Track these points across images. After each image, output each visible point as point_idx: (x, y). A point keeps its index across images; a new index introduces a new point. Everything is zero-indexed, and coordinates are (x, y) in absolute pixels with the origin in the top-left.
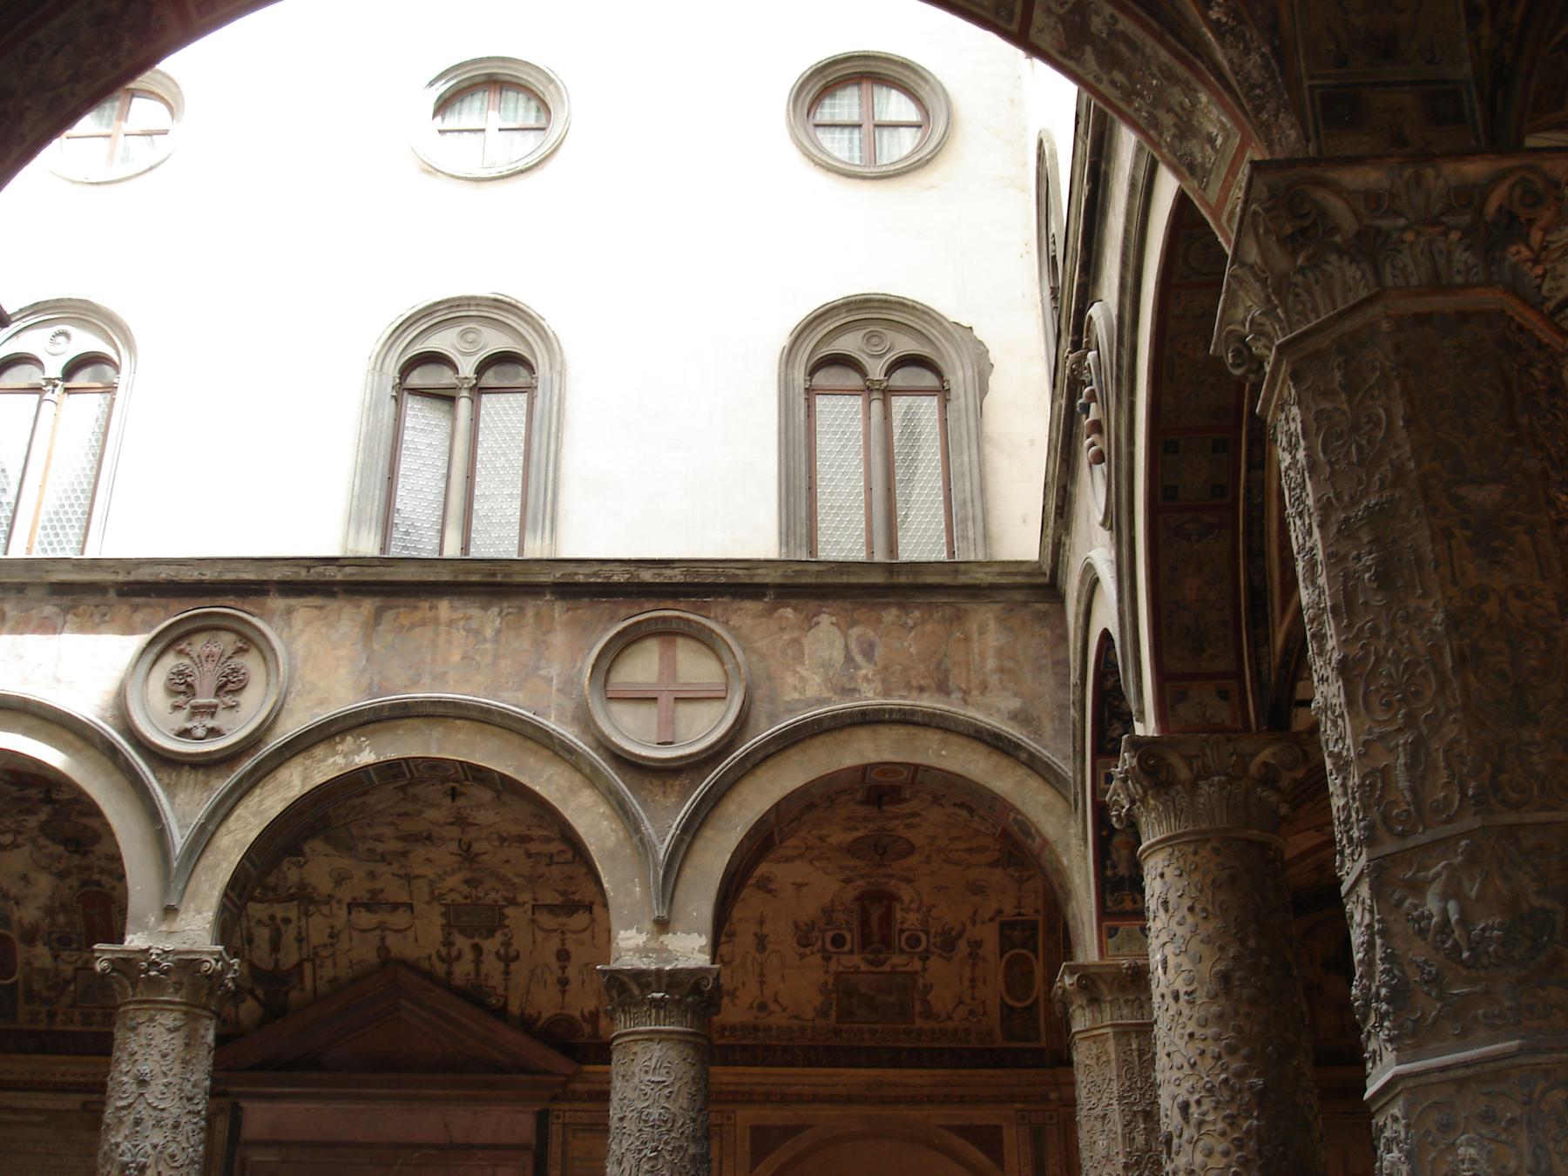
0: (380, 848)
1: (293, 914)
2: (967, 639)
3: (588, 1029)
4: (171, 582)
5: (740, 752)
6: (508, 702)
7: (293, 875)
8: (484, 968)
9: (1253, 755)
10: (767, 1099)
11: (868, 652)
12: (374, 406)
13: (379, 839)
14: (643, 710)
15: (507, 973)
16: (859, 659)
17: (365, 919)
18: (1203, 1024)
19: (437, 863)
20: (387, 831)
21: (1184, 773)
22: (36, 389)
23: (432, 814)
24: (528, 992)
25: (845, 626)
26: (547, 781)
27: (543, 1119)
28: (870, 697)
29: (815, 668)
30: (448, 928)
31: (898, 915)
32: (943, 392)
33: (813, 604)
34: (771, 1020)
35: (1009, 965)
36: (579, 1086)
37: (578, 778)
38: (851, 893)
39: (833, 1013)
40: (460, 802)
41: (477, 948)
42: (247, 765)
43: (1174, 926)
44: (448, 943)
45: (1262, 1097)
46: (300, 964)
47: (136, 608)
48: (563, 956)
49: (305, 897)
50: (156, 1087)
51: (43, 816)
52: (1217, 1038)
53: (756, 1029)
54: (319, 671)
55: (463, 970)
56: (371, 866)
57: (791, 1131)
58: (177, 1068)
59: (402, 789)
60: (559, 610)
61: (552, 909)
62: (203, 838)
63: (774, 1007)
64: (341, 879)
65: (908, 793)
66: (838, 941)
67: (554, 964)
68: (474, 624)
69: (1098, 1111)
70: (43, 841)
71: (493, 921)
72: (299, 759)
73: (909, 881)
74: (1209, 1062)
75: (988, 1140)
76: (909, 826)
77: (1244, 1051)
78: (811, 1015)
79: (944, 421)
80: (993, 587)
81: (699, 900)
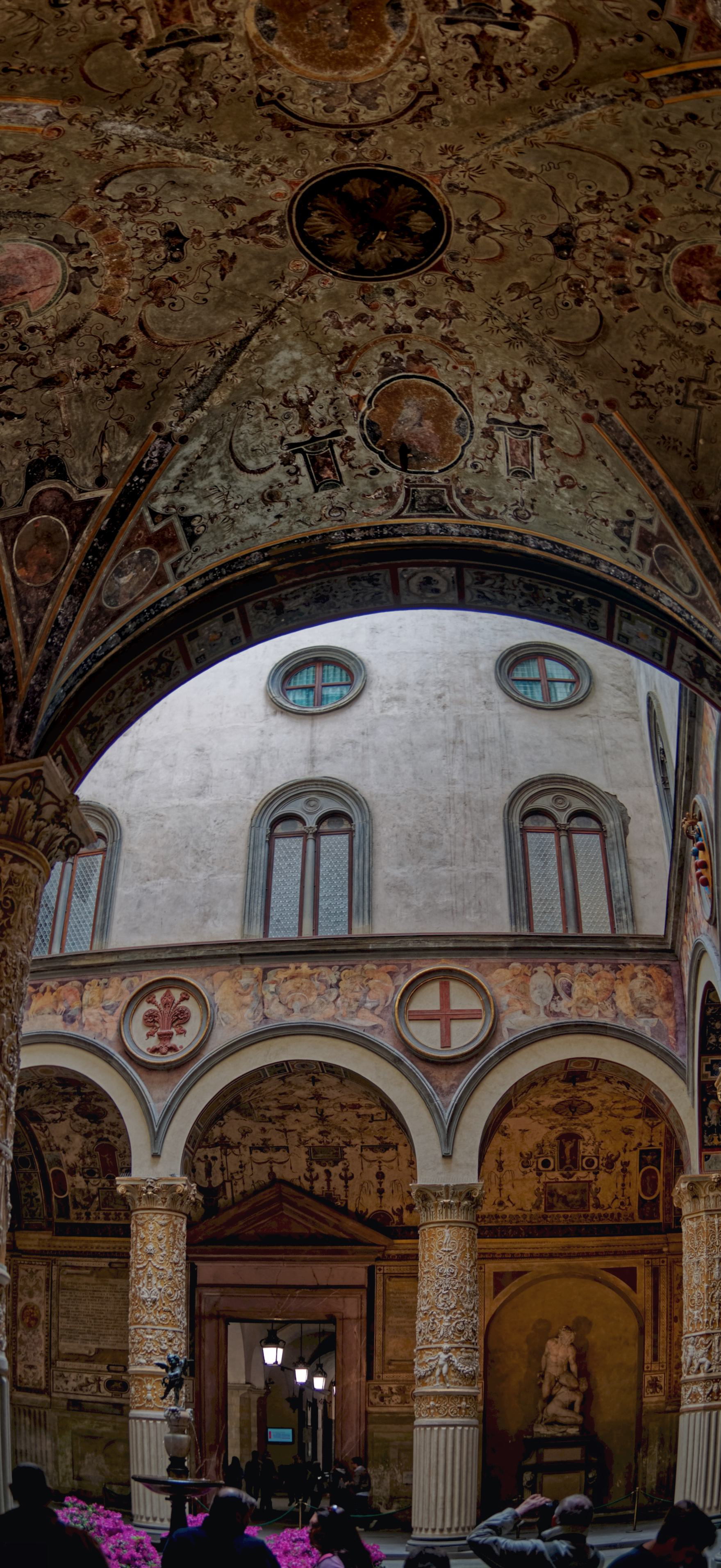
0: (268, 1114)
3: (396, 1219)
8: (332, 1184)
10: (503, 1257)
13: (267, 1108)
15: (346, 1187)
17: (260, 1156)
19: (303, 1122)
30: (310, 1161)
31: (581, 1147)
32: (602, 832)
34: (506, 1212)
36: (392, 1252)
38: (554, 1135)
41: (328, 1173)
44: (311, 1170)
48: (380, 1176)
49: (224, 1144)
53: (497, 1216)
55: (319, 1187)
56: (263, 1125)
61: (372, 1148)
62: (170, 1112)
63: (507, 1203)
64: (245, 1134)
65: (590, 1076)
66: (546, 1164)
67: (375, 1180)
71: (337, 1156)
76: (590, 1095)
78: (529, 1207)
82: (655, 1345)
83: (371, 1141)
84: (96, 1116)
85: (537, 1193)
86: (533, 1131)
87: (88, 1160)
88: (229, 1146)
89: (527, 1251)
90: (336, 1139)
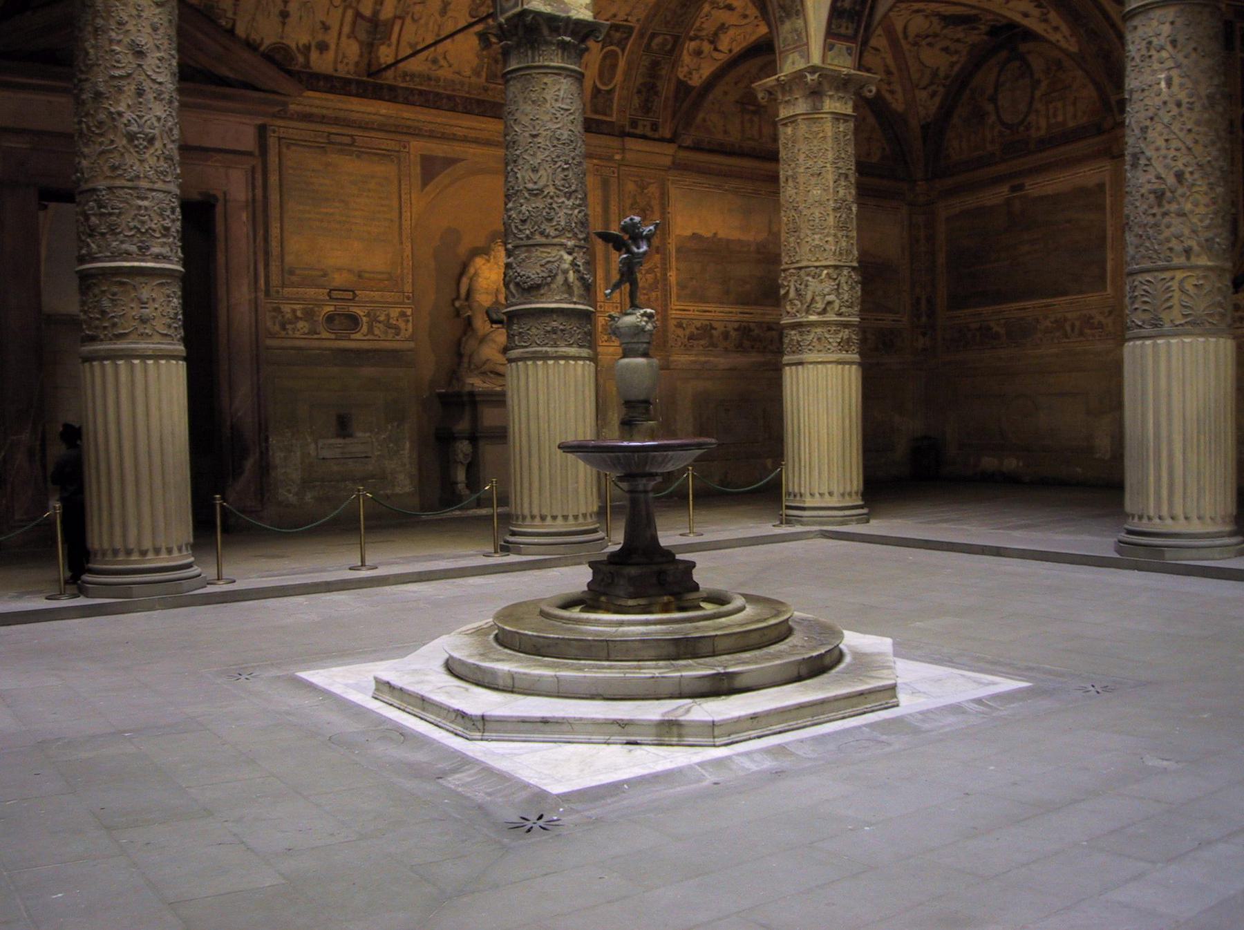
10: (432, 136)
24: (253, 19)
27: (262, 131)
34: (440, 73)
35: (604, 58)
39: (484, 74)
43: (1180, 57)
50: (151, 61)
52: (1206, 134)
53: (429, 79)
57: (450, 162)
63: (443, 62)
69: (815, 169)
89: (473, 134)
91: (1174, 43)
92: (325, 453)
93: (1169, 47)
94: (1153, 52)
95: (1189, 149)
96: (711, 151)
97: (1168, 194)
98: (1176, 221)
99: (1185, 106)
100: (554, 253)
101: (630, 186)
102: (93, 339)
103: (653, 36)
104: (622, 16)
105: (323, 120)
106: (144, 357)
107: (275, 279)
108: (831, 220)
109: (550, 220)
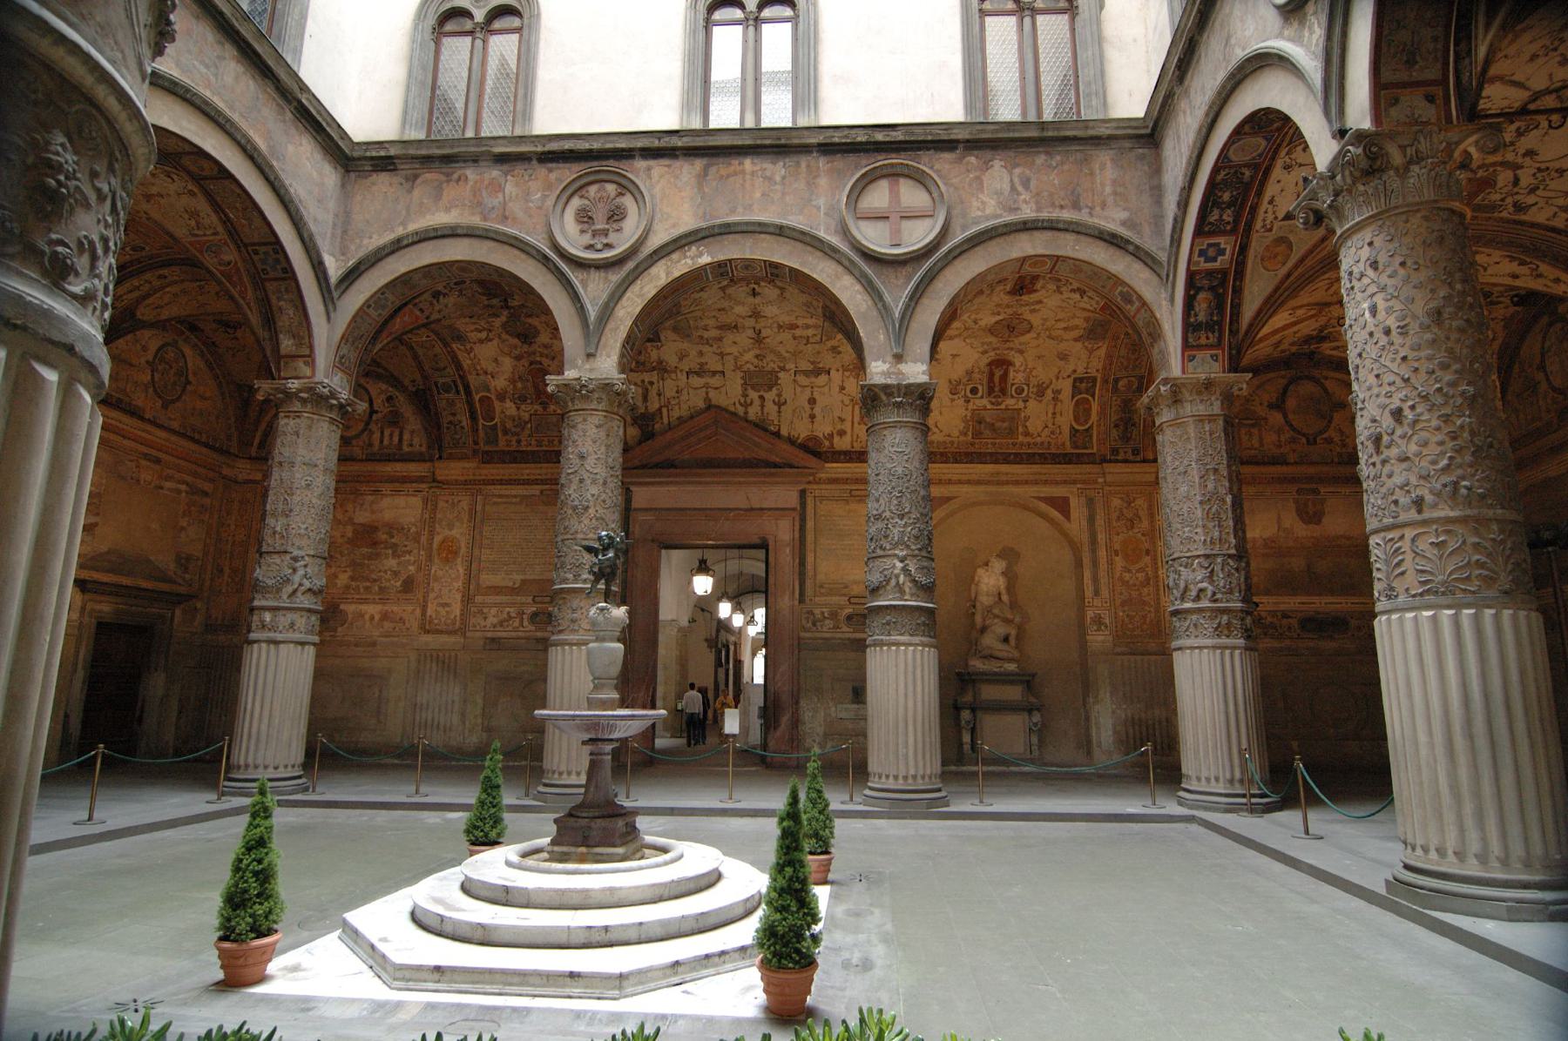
0: (706, 335)
1: (655, 379)
2: (1092, 174)
4: (571, 151)
5: (945, 249)
6: (795, 221)
7: (654, 354)
9: (1458, 143)
11: (1026, 183)
12: (694, 32)
14: (881, 224)
16: (1020, 188)
17: (696, 381)
18: (1417, 348)
19: (739, 345)
20: (712, 322)
21: (1397, 158)
22: (471, 33)
23: (739, 310)
25: (1010, 167)
26: (822, 270)
27: (803, 493)
28: (1028, 212)
29: (991, 194)
31: (1011, 374)
33: (988, 154)
37: (840, 269)
38: (985, 360)
40: (758, 300)
41: (762, 397)
42: (630, 265)
43: (1384, 279)
44: (745, 396)
45: (1472, 401)
46: (660, 409)
47: (551, 171)
48: (812, 401)
50: (591, 461)
51: (504, 319)
52: (1430, 358)
54: (671, 203)
55: (754, 412)
57: (949, 499)
58: (603, 449)
59: (723, 289)
60: (822, 162)
61: (806, 373)
62: (607, 312)
66: (974, 391)
67: (807, 406)
68: (768, 173)
69: (1181, 469)
70: (504, 336)
71: (771, 381)
72: (663, 261)
73: (1021, 352)
74: (1423, 376)
75: (1062, 505)
77: (1457, 366)
79: (1073, 30)
80: (1110, 138)
81: (920, 342)
82: (1095, 580)
83: (805, 366)
84: (527, 336)
85: (965, 420)
86: (967, 355)
87: (519, 385)
88: (666, 371)
89: (955, 477)
90: (771, 364)
91: (1374, 265)
92: (843, 715)
93: (1370, 272)
94: (1355, 282)
95: (1407, 381)
96: (1264, 464)
97: (1386, 438)
98: (1399, 468)
99: (1394, 333)
100: (888, 561)
101: (1116, 502)
102: (560, 632)
103: (1116, 381)
104: (1080, 370)
105: (846, 481)
106: (571, 644)
107: (809, 591)
108: (1199, 513)
109: (886, 537)
